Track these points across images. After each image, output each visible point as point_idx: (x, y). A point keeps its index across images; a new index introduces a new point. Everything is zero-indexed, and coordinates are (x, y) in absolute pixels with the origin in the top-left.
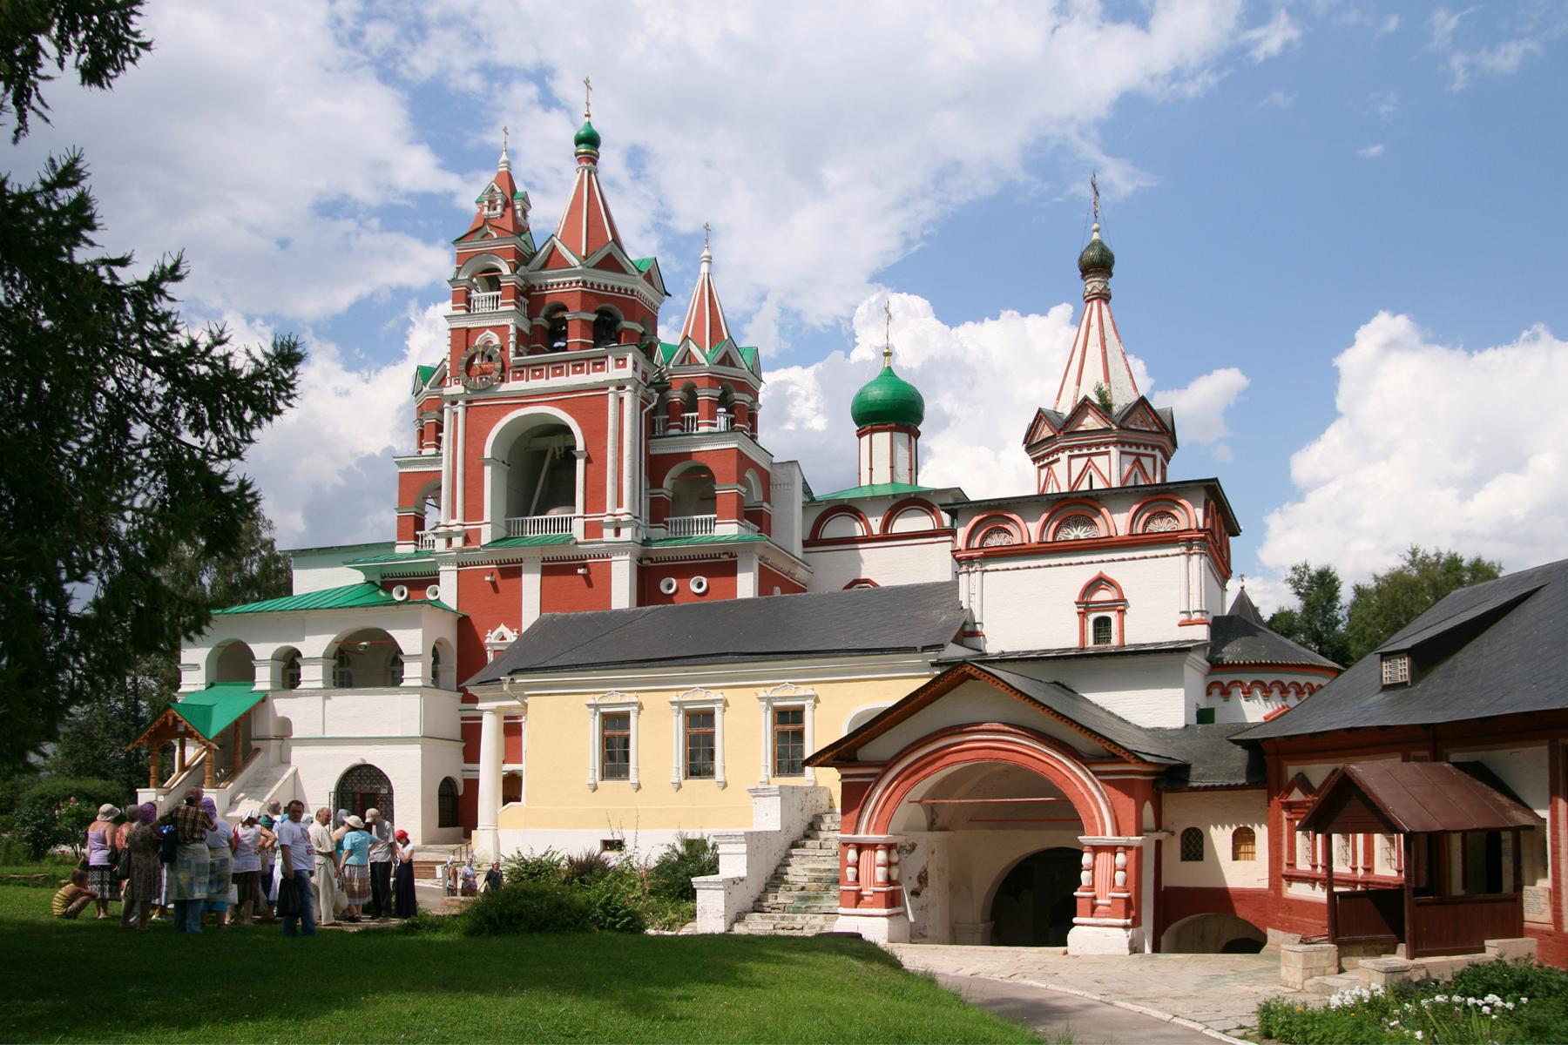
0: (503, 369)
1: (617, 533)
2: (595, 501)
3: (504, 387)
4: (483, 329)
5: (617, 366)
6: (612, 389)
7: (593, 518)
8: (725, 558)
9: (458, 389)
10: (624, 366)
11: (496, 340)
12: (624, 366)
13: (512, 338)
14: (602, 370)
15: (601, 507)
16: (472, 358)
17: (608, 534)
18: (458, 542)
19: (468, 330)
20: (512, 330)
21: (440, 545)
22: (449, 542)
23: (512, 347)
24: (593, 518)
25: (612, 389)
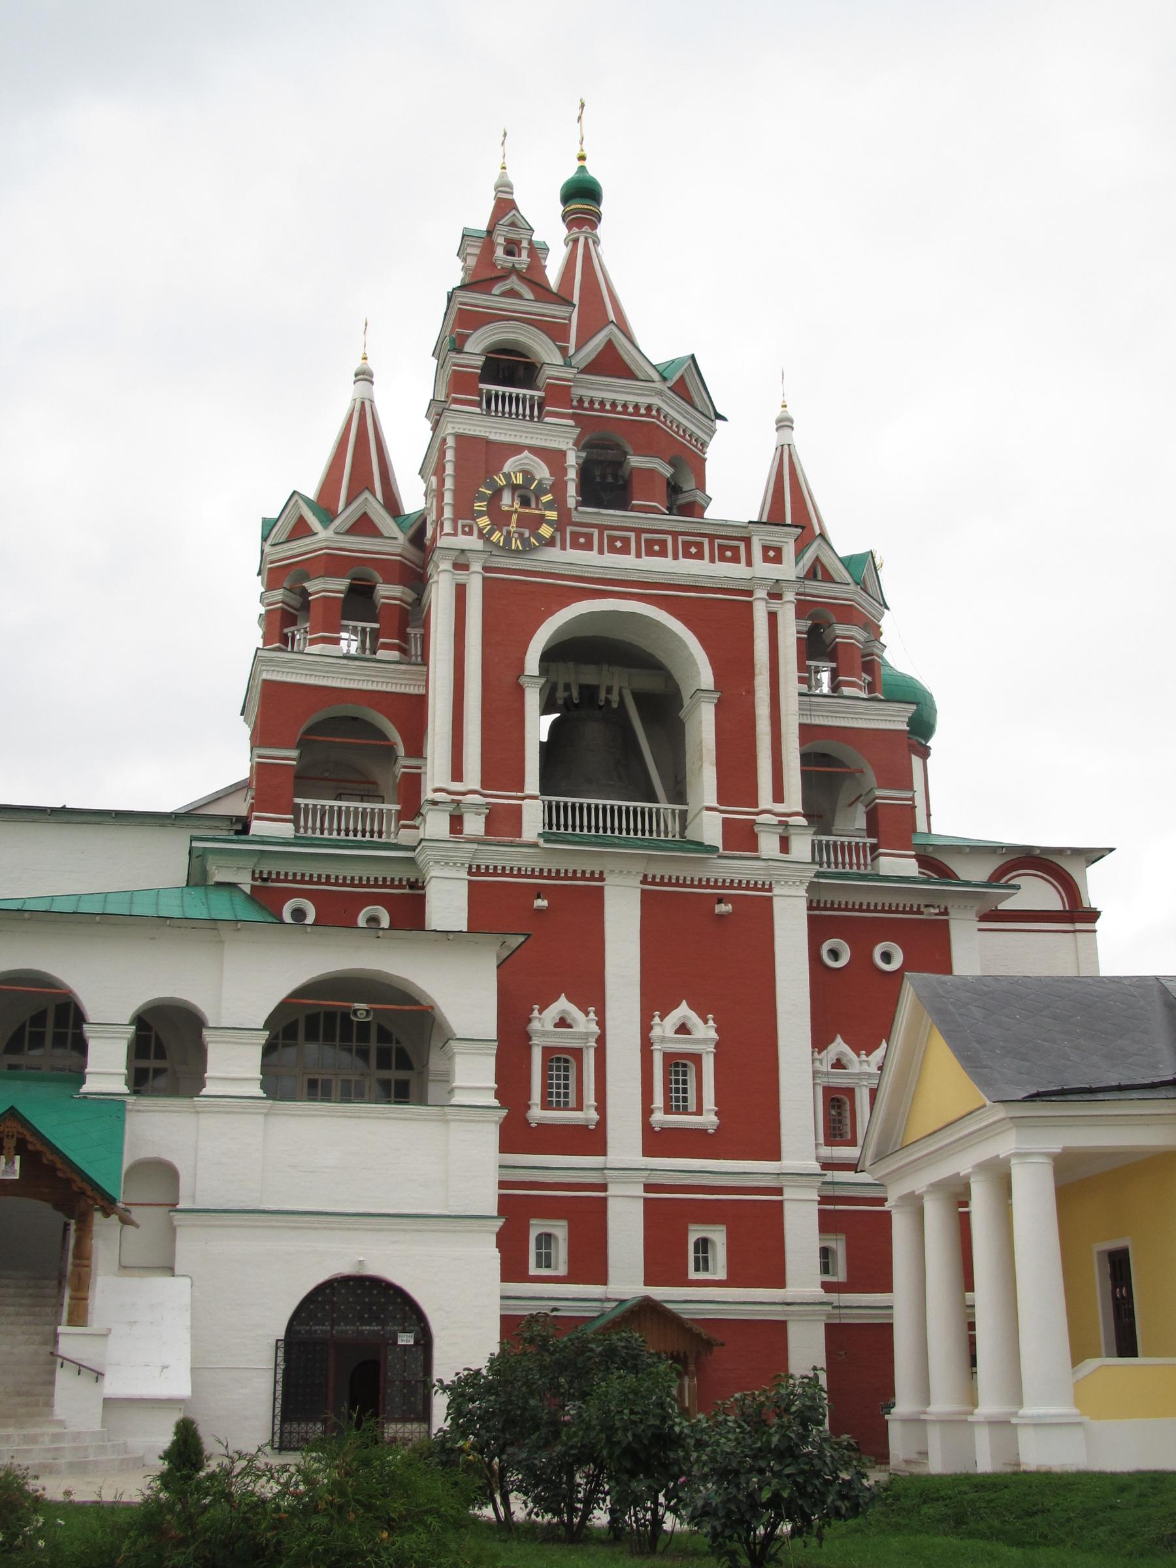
0: (559, 526)
1: (785, 845)
2: (737, 783)
3: (554, 555)
4: (517, 449)
5: (766, 559)
6: (761, 593)
7: (739, 814)
8: (931, 913)
9: (473, 542)
10: (778, 559)
11: (542, 472)
12: (778, 559)
13: (572, 474)
14: (736, 559)
15: (750, 797)
16: (498, 492)
17: (768, 844)
18: (474, 825)
19: (488, 443)
20: (572, 459)
21: (436, 824)
22: (456, 822)
23: (572, 489)
24: (739, 814)
25: (761, 593)
